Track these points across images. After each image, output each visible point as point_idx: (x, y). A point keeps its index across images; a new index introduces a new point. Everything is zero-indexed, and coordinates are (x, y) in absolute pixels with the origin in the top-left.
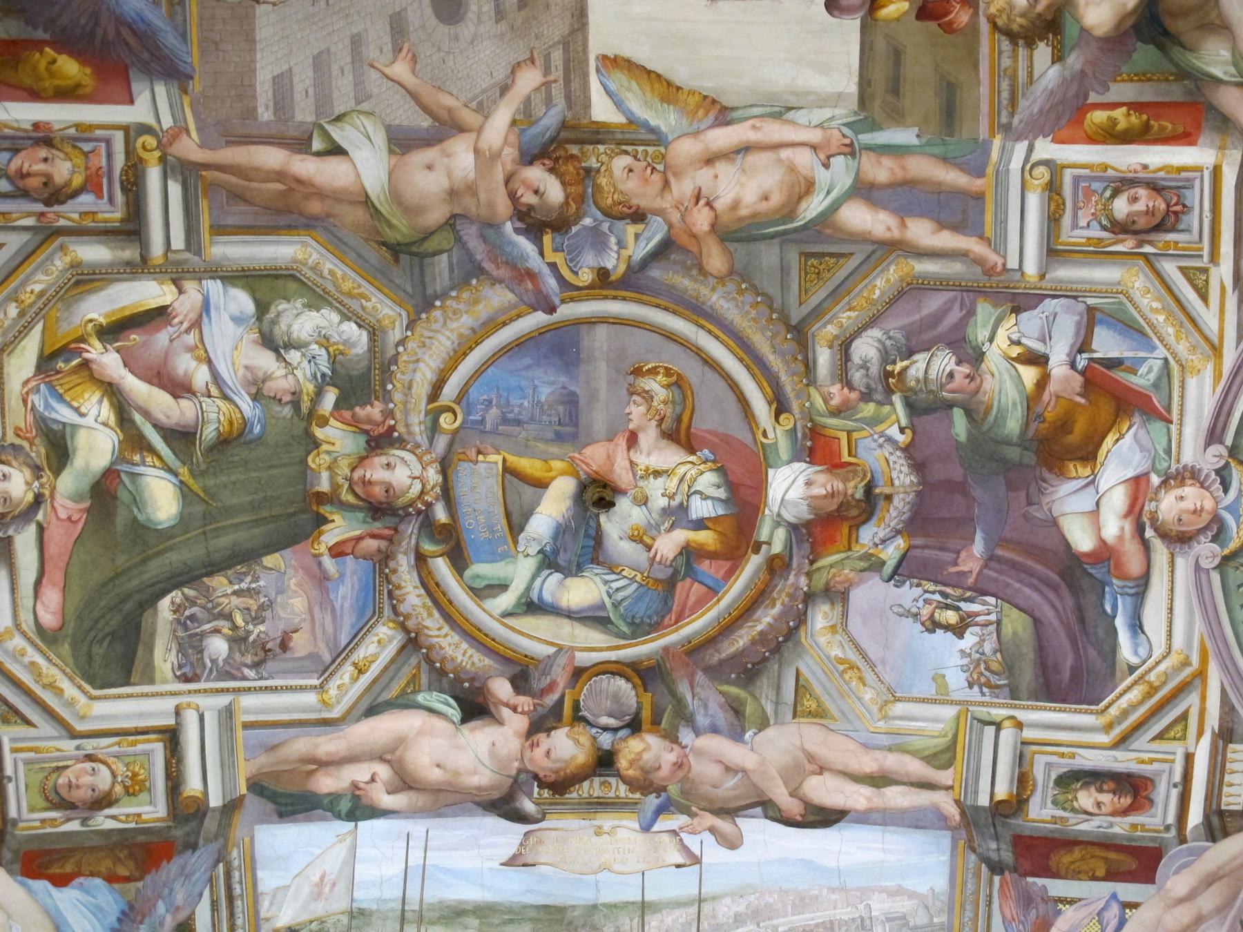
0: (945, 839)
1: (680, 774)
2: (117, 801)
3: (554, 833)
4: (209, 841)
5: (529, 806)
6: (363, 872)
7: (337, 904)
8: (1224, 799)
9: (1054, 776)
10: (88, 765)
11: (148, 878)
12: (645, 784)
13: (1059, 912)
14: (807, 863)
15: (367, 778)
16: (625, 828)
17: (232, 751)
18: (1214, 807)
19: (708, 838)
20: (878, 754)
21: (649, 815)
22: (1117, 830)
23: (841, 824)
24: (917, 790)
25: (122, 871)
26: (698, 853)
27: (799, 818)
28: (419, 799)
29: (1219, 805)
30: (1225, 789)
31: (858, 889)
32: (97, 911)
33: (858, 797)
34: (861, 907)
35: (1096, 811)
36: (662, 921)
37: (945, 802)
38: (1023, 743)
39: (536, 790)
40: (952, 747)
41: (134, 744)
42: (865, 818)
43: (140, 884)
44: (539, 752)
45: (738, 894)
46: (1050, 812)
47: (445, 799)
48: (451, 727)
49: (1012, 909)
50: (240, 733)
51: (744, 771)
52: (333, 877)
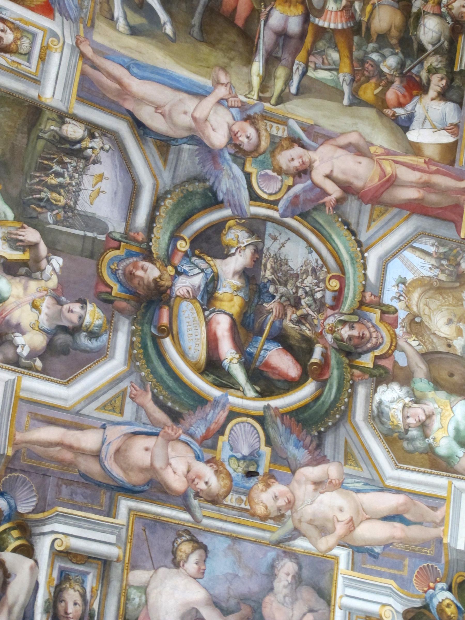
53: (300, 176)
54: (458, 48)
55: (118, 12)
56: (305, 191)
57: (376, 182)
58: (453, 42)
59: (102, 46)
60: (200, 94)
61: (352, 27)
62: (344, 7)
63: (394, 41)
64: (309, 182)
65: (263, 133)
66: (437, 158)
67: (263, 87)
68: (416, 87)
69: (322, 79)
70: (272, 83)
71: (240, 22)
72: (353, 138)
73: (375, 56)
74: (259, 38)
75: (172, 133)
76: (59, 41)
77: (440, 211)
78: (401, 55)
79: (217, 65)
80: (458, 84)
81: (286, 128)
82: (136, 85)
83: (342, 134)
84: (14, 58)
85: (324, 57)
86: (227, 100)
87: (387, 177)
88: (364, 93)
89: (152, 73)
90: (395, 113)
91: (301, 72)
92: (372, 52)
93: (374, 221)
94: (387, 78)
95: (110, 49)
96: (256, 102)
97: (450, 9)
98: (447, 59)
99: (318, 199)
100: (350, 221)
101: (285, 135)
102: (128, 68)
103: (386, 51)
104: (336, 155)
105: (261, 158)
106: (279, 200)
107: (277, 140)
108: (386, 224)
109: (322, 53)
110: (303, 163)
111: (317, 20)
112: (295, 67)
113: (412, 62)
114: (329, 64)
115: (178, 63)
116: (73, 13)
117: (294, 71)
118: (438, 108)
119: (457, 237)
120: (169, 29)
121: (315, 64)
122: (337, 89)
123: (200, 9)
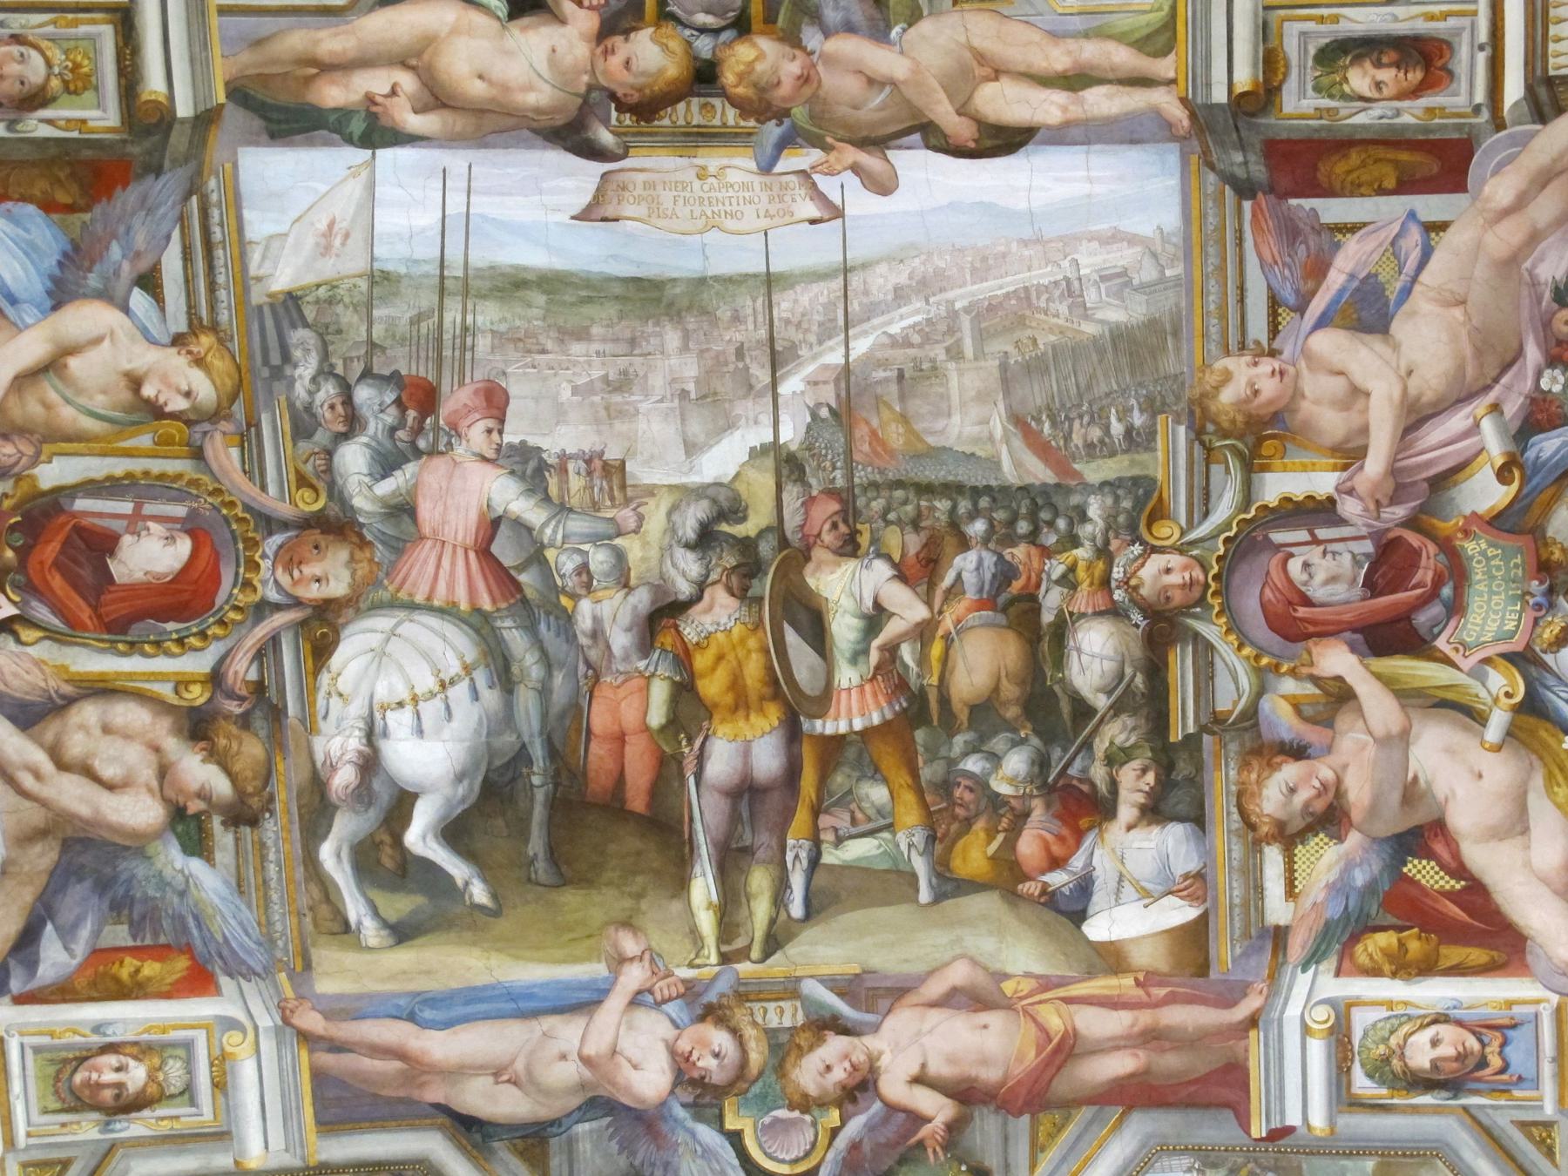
0: (1171, 155)
1: (807, 91)
2: (54, 99)
3: (641, 177)
4: (175, 163)
5: (605, 137)
6: (388, 221)
7: (350, 263)
8: (1551, 61)
9: (1312, 51)
10: (15, 49)
11: (98, 210)
12: (761, 107)
13: (1337, 246)
14: (988, 208)
15: (386, 90)
16: (738, 166)
17: (205, 45)
18: (1539, 72)
19: (850, 179)
20: (1071, 44)
21: (769, 150)
22: (1407, 119)
23: (1029, 147)
24: (1128, 89)
25: (62, 197)
26: (838, 202)
27: (972, 145)
28: (459, 123)
29: (1545, 69)
30: (1552, 47)
31: (1061, 238)
32: (30, 250)
33: (1048, 107)
34: (1066, 263)
35: (1376, 95)
36: (796, 301)
37: (1166, 102)
38: (1266, 8)
39: (614, 114)
40: (1170, 24)
41: (76, 24)
42: (1061, 135)
43: (87, 217)
44: (616, 61)
45: (896, 258)
46: (1312, 102)
47: (491, 123)
48: (496, 24)
49: (1272, 247)
50: (214, 20)
51: (894, 83)
52: (344, 224)
53: (854, 1100)
54: (1170, 680)
55: (355, 908)
56: (871, 1128)
57: (1031, 1057)
58: (1156, 670)
59: (340, 997)
60: (584, 1002)
61: (905, 710)
62: (877, 668)
63: (1012, 712)
64: (877, 1106)
65: (749, 1032)
66: (1162, 965)
67: (728, 926)
68: (1084, 809)
69: (859, 859)
70: (744, 912)
71: (637, 801)
72: (959, 974)
73: (973, 764)
74: (691, 819)
75: (544, 1112)
76: (244, 1031)
77: (1192, 1089)
78: (1035, 741)
79: (607, 924)
80: (1186, 772)
81: (798, 1004)
82: (439, 1046)
83: (931, 973)
84: (161, 1111)
85: (853, 806)
86: (650, 991)
87: (1055, 1041)
88: (964, 859)
89: (467, 1003)
90: (1045, 884)
91: (805, 863)
92: (965, 754)
93: (1043, 1150)
94: (1012, 809)
95: (360, 997)
96: (717, 969)
97: (1136, 588)
98: (1147, 719)
99: (906, 1137)
100: (986, 1164)
101: (800, 1019)
102: (412, 1018)
103: (998, 743)
104: (926, 1027)
105: (756, 1089)
106: (817, 1168)
107: (784, 1038)
108: (1072, 1148)
109: (847, 798)
110: (855, 1068)
111: (818, 723)
112: (789, 857)
113: (1065, 750)
114: (869, 819)
115: (518, 958)
116: (257, 960)
117: (789, 865)
118: (1145, 844)
119: (1245, 1140)
120: (479, 893)
121: (836, 830)
122: (899, 872)
123: (539, 813)
